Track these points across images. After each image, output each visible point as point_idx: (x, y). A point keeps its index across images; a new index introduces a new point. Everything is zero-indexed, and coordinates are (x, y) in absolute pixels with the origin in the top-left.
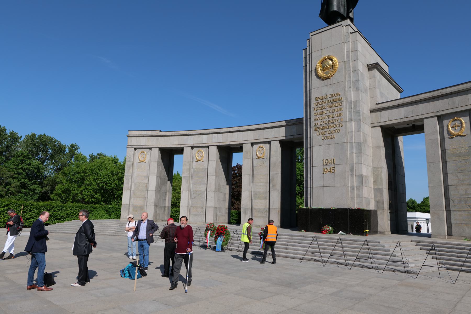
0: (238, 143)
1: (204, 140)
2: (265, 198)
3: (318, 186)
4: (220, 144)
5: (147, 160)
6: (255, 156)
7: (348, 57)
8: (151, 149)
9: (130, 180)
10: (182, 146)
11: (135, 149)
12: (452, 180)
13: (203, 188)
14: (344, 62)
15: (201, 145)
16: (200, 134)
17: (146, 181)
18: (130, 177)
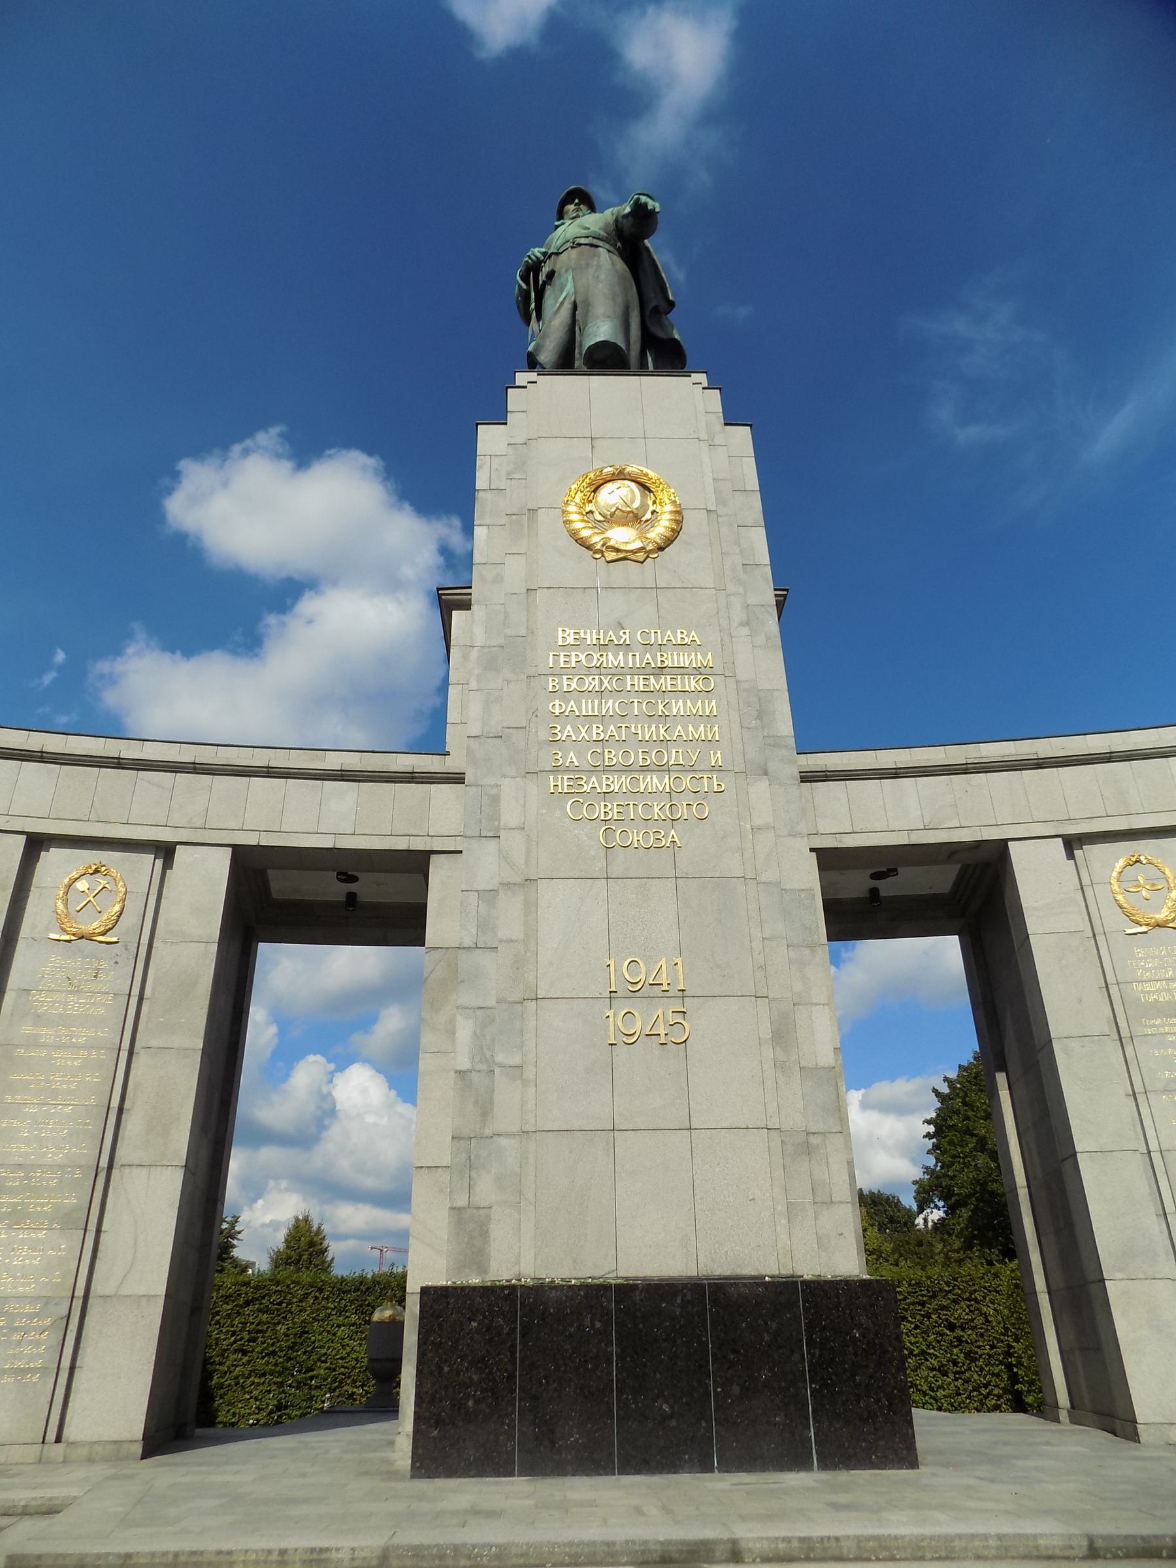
2: (65, 1221)
3: (577, 1124)
14: (708, 511)
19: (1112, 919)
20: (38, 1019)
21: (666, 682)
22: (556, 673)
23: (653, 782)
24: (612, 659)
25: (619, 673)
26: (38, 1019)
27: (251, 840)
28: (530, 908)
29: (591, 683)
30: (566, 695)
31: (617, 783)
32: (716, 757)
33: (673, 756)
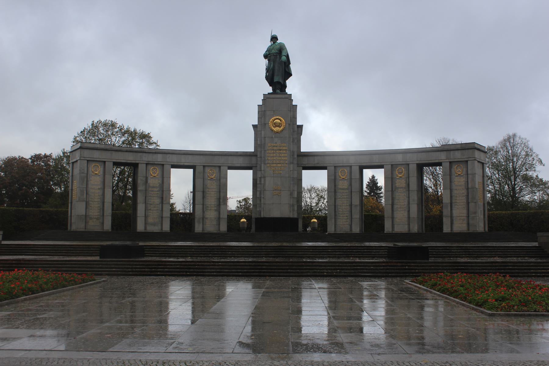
0: (192, 164)
1: (159, 158)
2: (216, 210)
4: (175, 164)
5: (102, 173)
6: (207, 176)
7: (291, 121)
8: (105, 162)
9: (85, 192)
10: (137, 162)
11: (88, 161)
12: (339, 202)
13: (157, 201)
15: (156, 163)
16: (155, 153)
17: (101, 193)
18: (85, 189)
19: (338, 177)
20: (209, 189)
21: (281, 151)
22: (268, 150)
23: (279, 165)
24: (275, 148)
25: (276, 150)
26: (209, 189)
27: (230, 165)
28: (265, 180)
29: (272, 152)
30: (269, 153)
31: (275, 165)
32: (286, 162)
33: (282, 162)
